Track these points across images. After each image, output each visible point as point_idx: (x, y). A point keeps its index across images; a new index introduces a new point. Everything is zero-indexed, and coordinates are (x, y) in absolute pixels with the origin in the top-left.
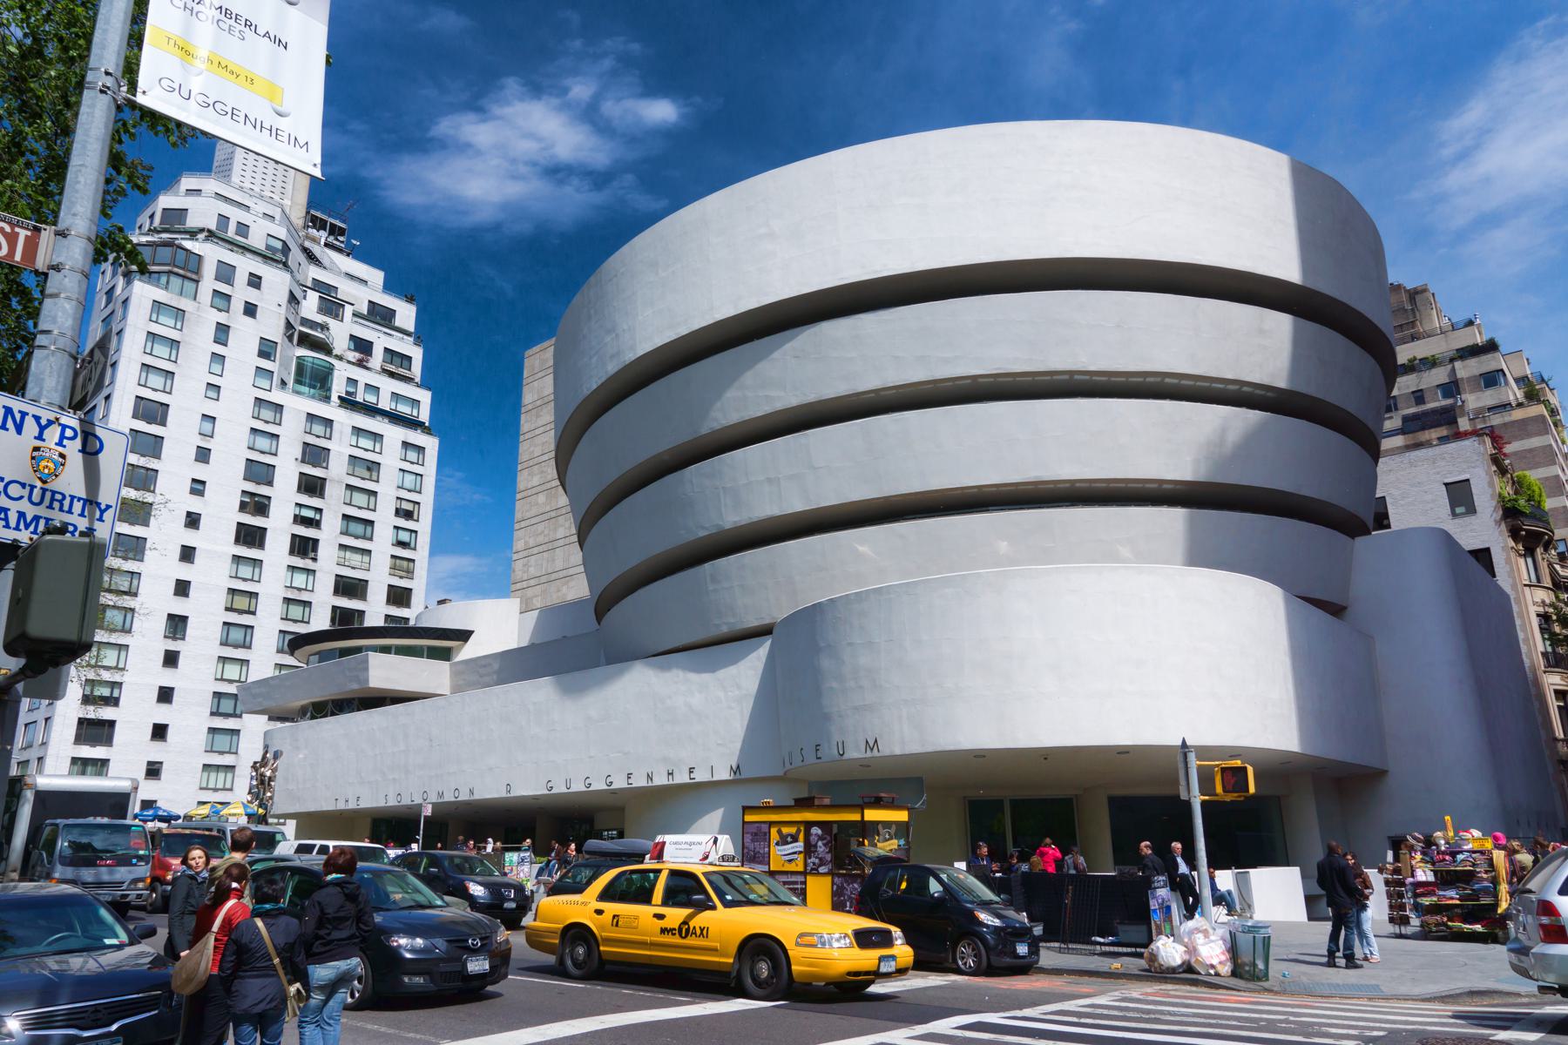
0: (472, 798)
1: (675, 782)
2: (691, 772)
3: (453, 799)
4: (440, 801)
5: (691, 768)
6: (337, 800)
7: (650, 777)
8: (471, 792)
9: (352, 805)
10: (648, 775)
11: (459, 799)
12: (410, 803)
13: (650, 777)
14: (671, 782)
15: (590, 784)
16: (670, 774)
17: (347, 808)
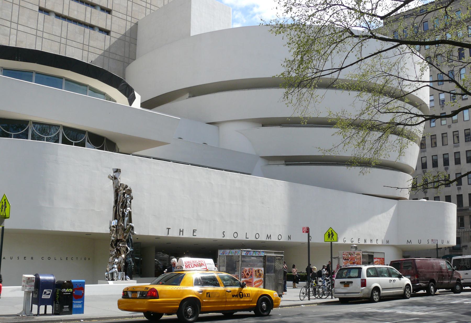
0: (289, 241)
1: (372, 244)
2: (377, 241)
3: (277, 240)
4: (268, 240)
5: (377, 239)
6: (169, 229)
7: (365, 241)
8: (289, 237)
9: (187, 235)
10: (365, 240)
11: (281, 240)
12: (244, 238)
13: (365, 241)
14: (371, 244)
15: (353, 241)
16: (371, 241)
17: (181, 236)
